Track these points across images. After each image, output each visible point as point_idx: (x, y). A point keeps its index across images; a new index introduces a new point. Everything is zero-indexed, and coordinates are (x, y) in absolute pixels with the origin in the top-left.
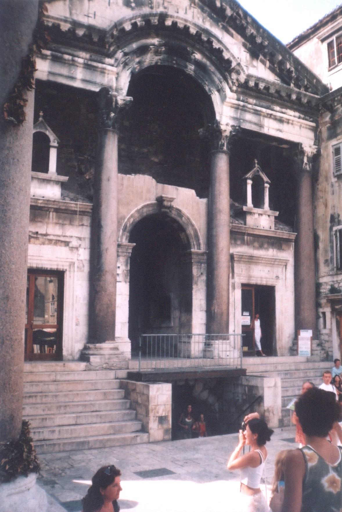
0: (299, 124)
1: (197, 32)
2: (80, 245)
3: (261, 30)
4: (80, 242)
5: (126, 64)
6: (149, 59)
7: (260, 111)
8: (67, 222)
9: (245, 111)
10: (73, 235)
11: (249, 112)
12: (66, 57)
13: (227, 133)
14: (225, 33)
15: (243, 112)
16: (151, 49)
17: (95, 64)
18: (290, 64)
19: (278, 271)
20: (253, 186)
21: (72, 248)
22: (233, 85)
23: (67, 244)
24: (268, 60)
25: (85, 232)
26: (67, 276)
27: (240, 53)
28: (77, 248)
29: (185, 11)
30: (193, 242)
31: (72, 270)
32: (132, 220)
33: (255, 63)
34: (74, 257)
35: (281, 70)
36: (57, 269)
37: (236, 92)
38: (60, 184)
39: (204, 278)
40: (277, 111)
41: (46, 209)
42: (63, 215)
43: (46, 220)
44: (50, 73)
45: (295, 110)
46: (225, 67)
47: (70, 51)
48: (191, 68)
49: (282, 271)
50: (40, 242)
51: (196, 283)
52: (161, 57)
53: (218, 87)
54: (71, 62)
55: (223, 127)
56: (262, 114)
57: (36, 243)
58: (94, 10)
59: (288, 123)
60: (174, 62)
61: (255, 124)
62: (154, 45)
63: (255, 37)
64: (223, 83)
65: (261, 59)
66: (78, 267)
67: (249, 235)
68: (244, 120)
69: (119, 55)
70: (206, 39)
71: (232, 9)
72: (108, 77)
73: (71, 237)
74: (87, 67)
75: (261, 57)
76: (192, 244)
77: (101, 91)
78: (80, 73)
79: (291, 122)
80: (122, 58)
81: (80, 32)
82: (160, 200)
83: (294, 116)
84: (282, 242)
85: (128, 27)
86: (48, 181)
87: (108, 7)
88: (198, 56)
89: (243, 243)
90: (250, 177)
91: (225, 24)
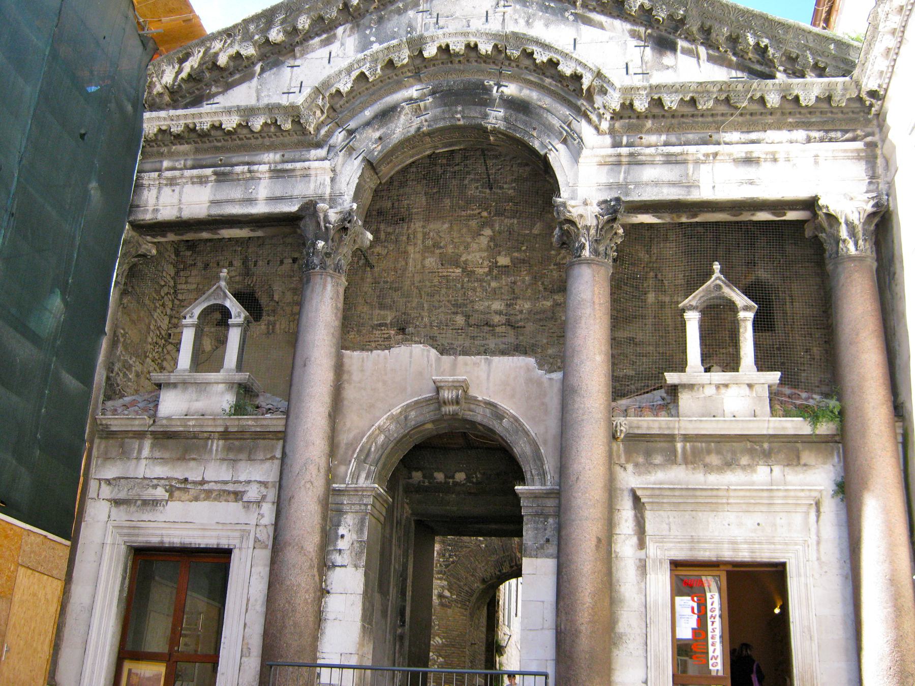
1: (495, 46)
2: (264, 497)
5: (350, 150)
6: (402, 127)
8: (243, 456)
10: (253, 479)
11: (652, 163)
12: (238, 169)
13: (591, 222)
14: (584, 28)
17: (289, 166)
18: (755, 34)
23: (237, 496)
24: (702, 44)
28: (258, 503)
29: (484, 19)
30: (528, 468)
31: (244, 545)
32: (382, 438)
33: (668, 59)
36: (218, 544)
40: (734, 141)
42: (237, 443)
43: (207, 457)
44: (214, 203)
45: (792, 127)
46: (573, 90)
47: (247, 159)
48: (496, 117)
49: (806, 523)
50: (190, 497)
53: (561, 133)
54: (248, 175)
56: (690, 158)
57: (183, 498)
59: (775, 160)
60: (459, 116)
61: (673, 184)
62: (410, 100)
63: (651, 9)
64: (575, 124)
65: (682, 48)
67: (686, 438)
68: (638, 184)
69: (339, 137)
70: (517, 54)
73: (249, 482)
74: (278, 174)
75: (681, 43)
77: (300, 209)
79: (781, 156)
81: (257, 124)
84: (799, 445)
85: (345, 86)
87: (328, 66)
89: (671, 459)
90: (694, 303)
91: (580, 11)
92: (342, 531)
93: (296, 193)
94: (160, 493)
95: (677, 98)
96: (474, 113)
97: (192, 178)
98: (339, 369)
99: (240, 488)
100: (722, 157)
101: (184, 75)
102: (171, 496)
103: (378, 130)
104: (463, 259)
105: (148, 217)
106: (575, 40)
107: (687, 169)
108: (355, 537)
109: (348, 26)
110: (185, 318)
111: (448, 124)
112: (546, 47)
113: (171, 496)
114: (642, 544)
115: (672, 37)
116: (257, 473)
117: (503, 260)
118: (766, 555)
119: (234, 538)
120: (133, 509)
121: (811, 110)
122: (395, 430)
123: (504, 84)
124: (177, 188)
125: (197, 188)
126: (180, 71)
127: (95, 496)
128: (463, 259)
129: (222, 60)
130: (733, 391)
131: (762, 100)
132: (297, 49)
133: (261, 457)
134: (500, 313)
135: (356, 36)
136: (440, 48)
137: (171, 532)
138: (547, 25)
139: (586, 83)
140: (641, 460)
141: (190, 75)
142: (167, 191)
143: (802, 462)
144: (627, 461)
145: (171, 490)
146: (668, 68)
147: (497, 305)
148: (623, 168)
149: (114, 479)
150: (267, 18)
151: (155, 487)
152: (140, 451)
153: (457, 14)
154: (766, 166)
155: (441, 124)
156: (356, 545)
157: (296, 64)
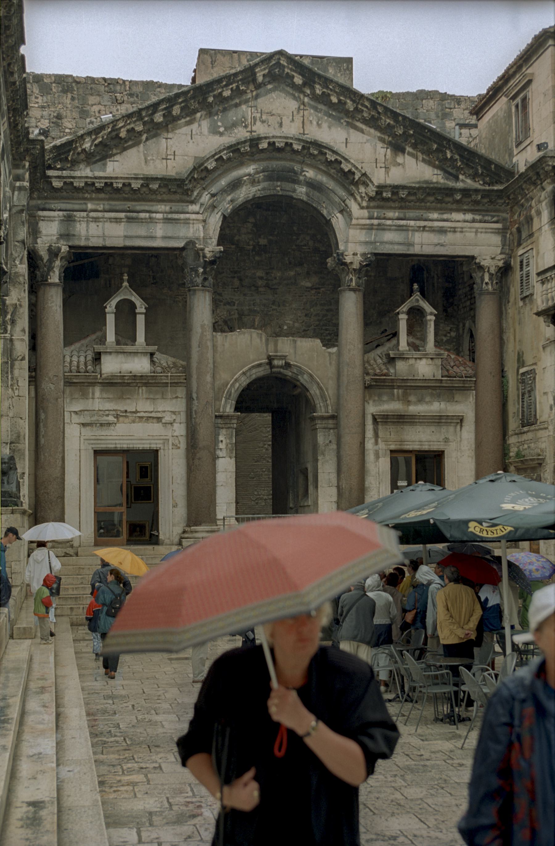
0: (474, 230)
3: (400, 118)
4: (174, 417)
5: (213, 207)
6: (245, 193)
7: (406, 226)
9: (384, 230)
11: (390, 230)
12: (142, 215)
13: (356, 266)
14: (352, 131)
15: (381, 232)
16: (245, 181)
18: (451, 151)
19: (449, 431)
20: (408, 320)
22: (362, 200)
23: (159, 419)
25: (180, 405)
26: (161, 454)
27: (375, 152)
29: (291, 117)
31: (166, 448)
32: (237, 385)
33: (400, 159)
34: (168, 433)
37: (368, 207)
38: (149, 355)
39: (334, 446)
41: (135, 384)
43: (136, 396)
45: (465, 211)
47: (147, 208)
48: (301, 191)
51: (323, 454)
55: (348, 260)
56: (410, 228)
58: (173, 149)
59: (455, 232)
62: (249, 175)
64: (347, 202)
66: (173, 444)
68: (382, 243)
69: (205, 198)
71: (354, 101)
72: (193, 227)
73: (164, 411)
74: (167, 220)
75: (408, 149)
76: (318, 406)
78: (159, 230)
80: (209, 200)
83: (465, 221)
85: (211, 165)
86: (136, 353)
87: (191, 141)
88: (310, 173)
89: (392, 398)
92: (221, 438)
93: (181, 234)
94: (111, 419)
95: (406, 192)
96: (288, 186)
97: (110, 218)
98: (214, 346)
99: (159, 415)
100: (427, 229)
101: (96, 142)
102: (118, 420)
103: (230, 194)
104: (236, 238)
105: (83, 243)
106: (346, 139)
107: (408, 235)
108: (228, 441)
109: (203, 113)
110: (106, 307)
111: (272, 193)
112: (334, 152)
113: (118, 420)
114: (376, 443)
115: (403, 144)
116: (171, 406)
117: (263, 241)
119: (159, 444)
120: (95, 429)
122: (245, 382)
123: (307, 170)
124: (100, 224)
125: (114, 225)
126: (95, 139)
127: (69, 421)
128: (236, 238)
129: (123, 134)
130: (424, 361)
132: (169, 126)
133: (170, 397)
134: (261, 278)
135: (208, 120)
136: (269, 143)
137: (121, 442)
138: (330, 127)
139: (357, 177)
140: (376, 398)
141: (101, 142)
142: (93, 225)
143: (456, 399)
144: (370, 399)
145: (117, 417)
147: (260, 273)
148: (374, 232)
149: (81, 411)
150: (155, 107)
151: (107, 415)
152: (93, 394)
153: (274, 112)
155: (268, 193)
156: (230, 446)
157: (169, 136)
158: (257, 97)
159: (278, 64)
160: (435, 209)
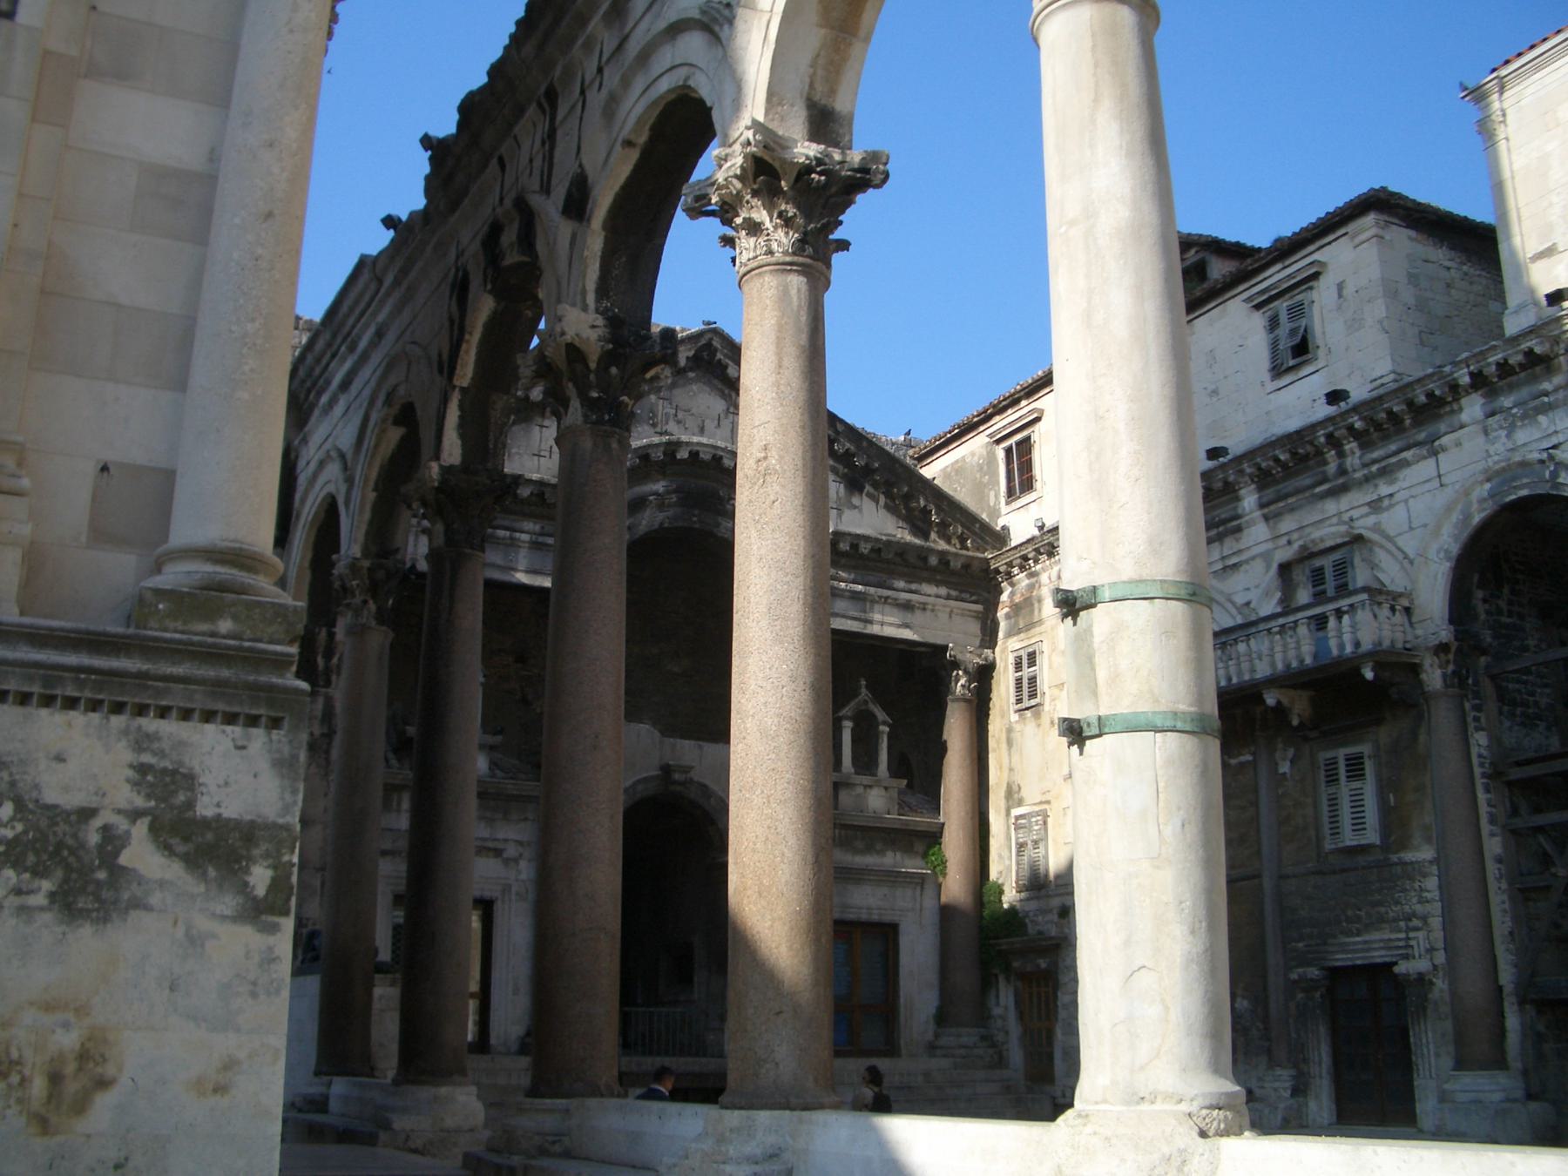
4: (521, 849)
6: (649, 520)
11: (842, 596)
12: (501, 533)
18: (926, 499)
21: (507, 862)
23: (498, 853)
26: (499, 909)
28: (516, 860)
33: (855, 500)
35: (909, 510)
45: (938, 584)
47: (506, 523)
52: (670, 513)
62: (656, 493)
73: (506, 840)
75: (868, 488)
82: (666, 770)
83: (938, 596)
95: (869, 546)
99: (500, 846)
118: (887, 918)
121: (953, 573)
131: (925, 559)
146: (855, 507)
152: (399, 804)
154: (918, 612)
155: (680, 524)
158: (673, 386)
159: (709, 345)
160: (901, 576)
